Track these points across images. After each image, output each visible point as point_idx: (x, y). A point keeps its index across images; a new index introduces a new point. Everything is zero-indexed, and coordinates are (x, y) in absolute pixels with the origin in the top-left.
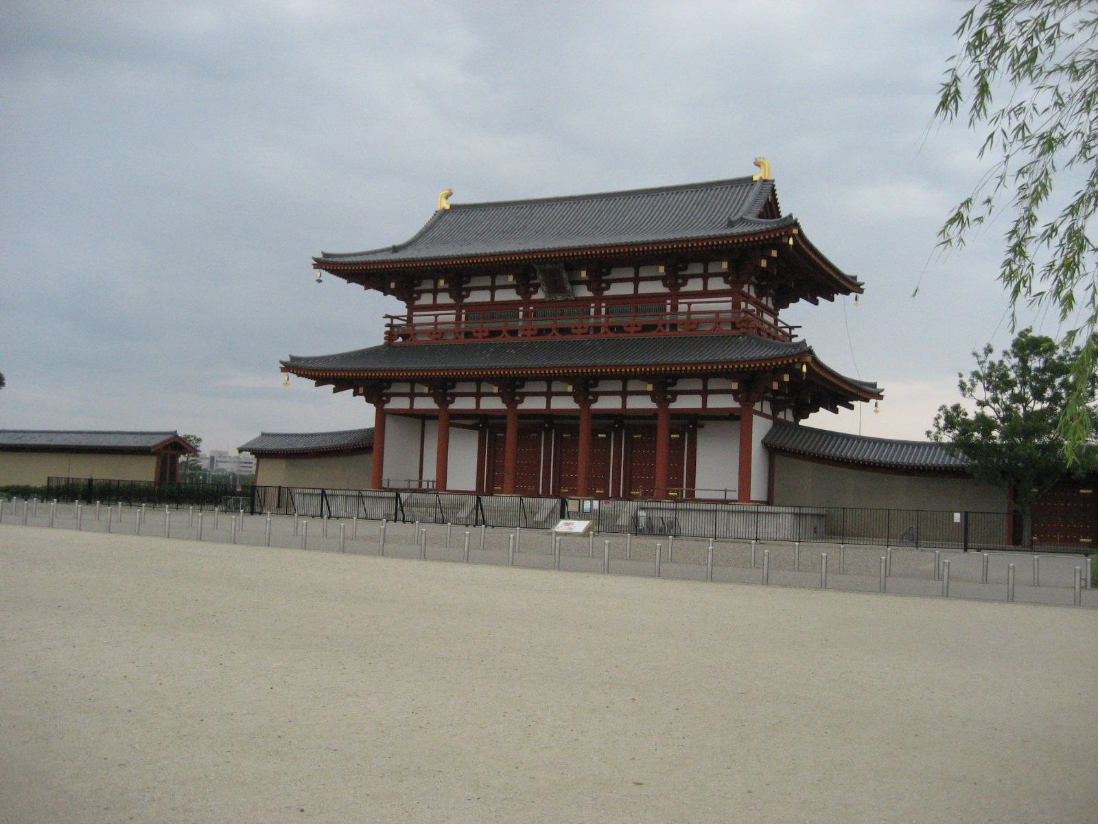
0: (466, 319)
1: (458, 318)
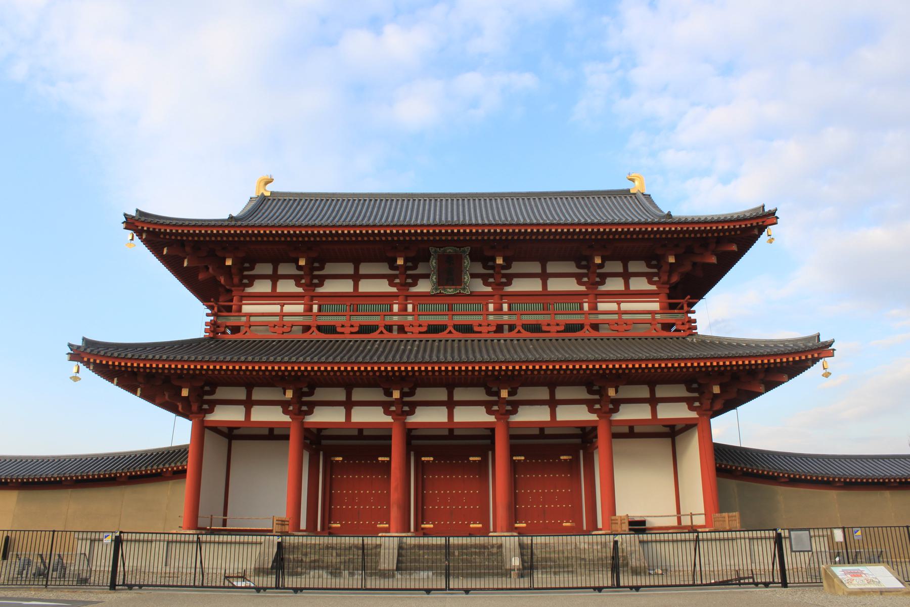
0: (320, 309)
1: (309, 309)
